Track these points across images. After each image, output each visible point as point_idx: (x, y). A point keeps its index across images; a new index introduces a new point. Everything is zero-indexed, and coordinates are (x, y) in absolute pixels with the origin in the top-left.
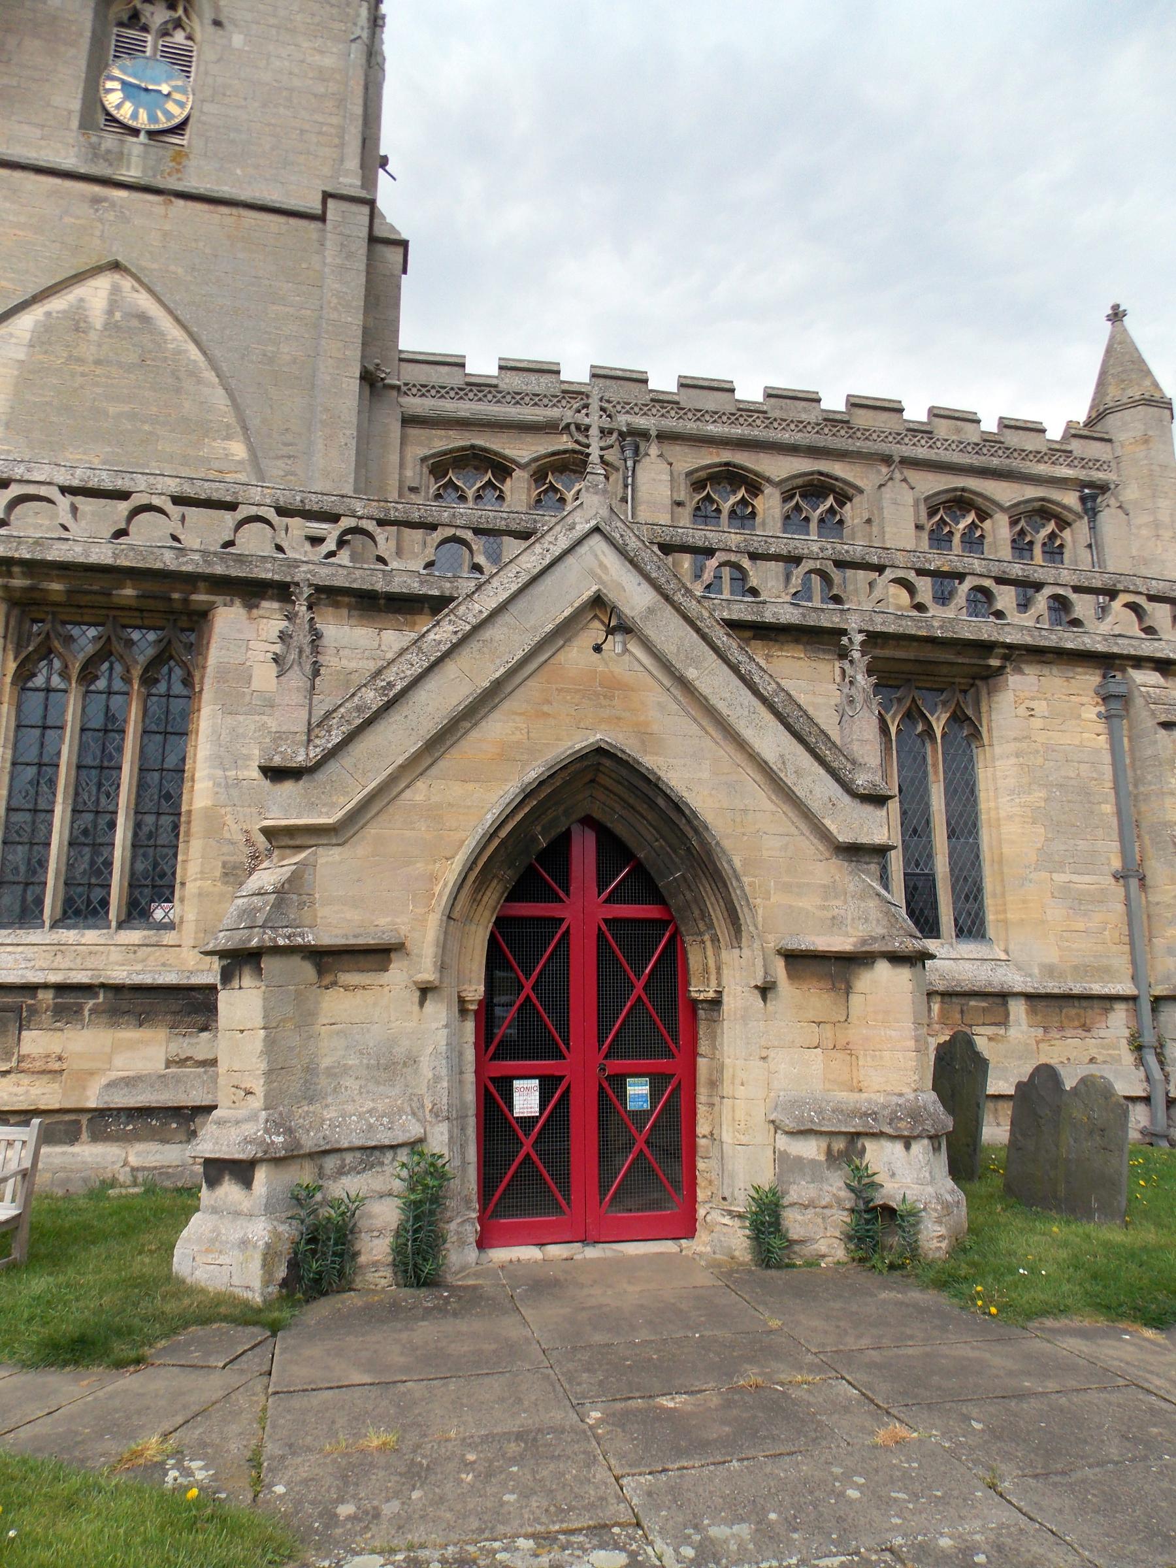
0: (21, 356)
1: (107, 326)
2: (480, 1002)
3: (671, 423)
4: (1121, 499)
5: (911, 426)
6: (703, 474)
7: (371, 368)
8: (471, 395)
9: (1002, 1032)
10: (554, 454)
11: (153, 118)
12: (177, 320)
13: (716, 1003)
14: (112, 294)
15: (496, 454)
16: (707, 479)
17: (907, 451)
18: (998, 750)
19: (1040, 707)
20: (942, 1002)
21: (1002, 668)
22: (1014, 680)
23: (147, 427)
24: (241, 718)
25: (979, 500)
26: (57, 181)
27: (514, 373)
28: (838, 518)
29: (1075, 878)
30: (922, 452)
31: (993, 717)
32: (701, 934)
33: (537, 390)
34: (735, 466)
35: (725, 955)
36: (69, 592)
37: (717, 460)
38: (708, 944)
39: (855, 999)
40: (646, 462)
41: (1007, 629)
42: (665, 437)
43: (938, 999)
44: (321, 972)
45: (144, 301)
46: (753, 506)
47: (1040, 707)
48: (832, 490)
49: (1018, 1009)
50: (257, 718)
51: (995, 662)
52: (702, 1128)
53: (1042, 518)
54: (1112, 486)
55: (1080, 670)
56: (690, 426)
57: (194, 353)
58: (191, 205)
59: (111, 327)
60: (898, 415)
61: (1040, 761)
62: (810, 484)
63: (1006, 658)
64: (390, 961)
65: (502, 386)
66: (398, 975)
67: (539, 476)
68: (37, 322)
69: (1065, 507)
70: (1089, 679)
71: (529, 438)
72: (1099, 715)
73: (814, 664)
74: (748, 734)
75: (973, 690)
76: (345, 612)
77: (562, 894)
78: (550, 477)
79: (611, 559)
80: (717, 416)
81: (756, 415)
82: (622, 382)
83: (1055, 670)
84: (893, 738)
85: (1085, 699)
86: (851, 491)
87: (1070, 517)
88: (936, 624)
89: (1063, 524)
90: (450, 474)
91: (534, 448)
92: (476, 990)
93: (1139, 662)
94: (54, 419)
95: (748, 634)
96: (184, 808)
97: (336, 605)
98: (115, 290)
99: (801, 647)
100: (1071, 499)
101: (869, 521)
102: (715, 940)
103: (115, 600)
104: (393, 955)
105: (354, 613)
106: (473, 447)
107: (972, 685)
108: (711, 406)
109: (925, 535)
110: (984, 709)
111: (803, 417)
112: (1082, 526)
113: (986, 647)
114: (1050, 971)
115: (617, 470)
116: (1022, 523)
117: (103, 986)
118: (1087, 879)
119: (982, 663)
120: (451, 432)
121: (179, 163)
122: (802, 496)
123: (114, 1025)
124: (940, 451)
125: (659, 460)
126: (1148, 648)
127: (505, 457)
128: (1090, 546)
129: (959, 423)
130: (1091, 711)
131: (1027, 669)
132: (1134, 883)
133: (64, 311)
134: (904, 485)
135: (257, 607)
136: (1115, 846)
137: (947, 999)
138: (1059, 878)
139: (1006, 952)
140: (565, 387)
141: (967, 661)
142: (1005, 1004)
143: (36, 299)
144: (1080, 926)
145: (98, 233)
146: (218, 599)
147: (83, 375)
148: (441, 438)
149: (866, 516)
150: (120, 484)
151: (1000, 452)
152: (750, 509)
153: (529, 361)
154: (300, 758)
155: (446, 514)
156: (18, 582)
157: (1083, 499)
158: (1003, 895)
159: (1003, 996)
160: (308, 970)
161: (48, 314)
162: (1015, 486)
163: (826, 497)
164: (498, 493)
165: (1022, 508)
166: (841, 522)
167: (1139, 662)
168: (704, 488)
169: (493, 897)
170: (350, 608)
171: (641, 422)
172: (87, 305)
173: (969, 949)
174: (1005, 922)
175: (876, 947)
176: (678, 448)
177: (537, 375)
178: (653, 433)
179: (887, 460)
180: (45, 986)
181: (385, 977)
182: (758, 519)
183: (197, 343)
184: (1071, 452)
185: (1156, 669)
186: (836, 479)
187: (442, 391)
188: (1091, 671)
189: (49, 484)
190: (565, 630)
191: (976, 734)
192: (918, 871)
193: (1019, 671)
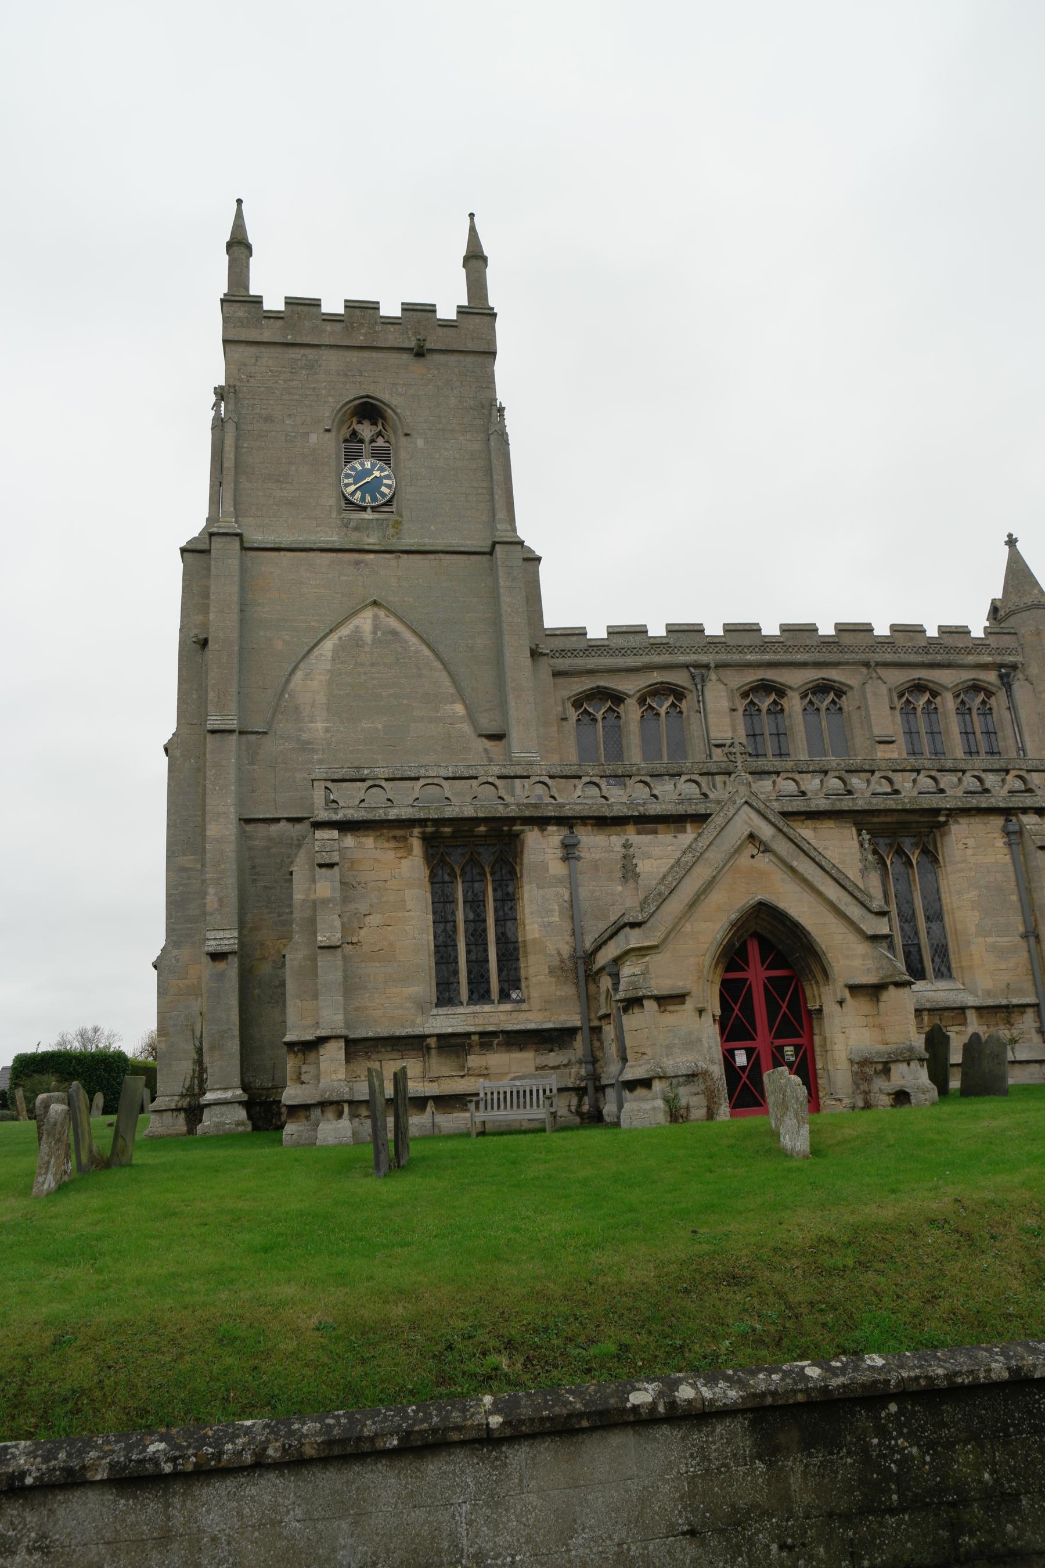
0: (329, 667)
1: (374, 640)
2: (720, 1016)
3: (723, 657)
4: (1027, 673)
5: (880, 640)
6: (747, 688)
7: (534, 647)
8: (593, 653)
9: (964, 1029)
10: (650, 686)
11: (374, 499)
12: (414, 632)
13: (820, 1011)
14: (373, 621)
15: (613, 690)
16: (750, 690)
18: (949, 869)
19: (971, 842)
20: (929, 1015)
21: (946, 823)
23: (405, 702)
24: (546, 890)
25: (931, 685)
26: (334, 555)
27: (618, 635)
28: (838, 706)
29: (999, 939)
30: (889, 657)
31: (945, 850)
32: (810, 981)
33: (634, 645)
34: (767, 680)
35: (822, 989)
36: (453, 832)
37: (755, 678)
38: (814, 985)
39: (882, 1005)
40: (709, 686)
41: (947, 799)
43: (926, 1013)
44: (659, 1006)
45: (393, 623)
46: (782, 705)
47: (971, 842)
48: (832, 688)
49: (971, 1015)
50: (554, 889)
51: (942, 819)
52: (819, 1065)
53: (975, 691)
54: (1020, 666)
55: (991, 818)
56: (736, 657)
57: (427, 652)
58: (411, 556)
59: (376, 641)
61: (973, 874)
62: (818, 686)
63: (947, 816)
64: (685, 1000)
65: (612, 645)
66: (689, 1005)
67: (642, 701)
68: (334, 645)
69: (989, 683)
70: (999, 821)
71: (632, 677)
72: (1005, 843)
73: (841, 831)
74: (822, 888)
75: (932, 834)
76: (589, 828)
77: (765, 966)
78: (648, 700)
79: (754, 815)
81: (777, 645)
82: (688, 633)
83: (977, 819)
84: (889, 867)
85: (996, 835)
86: (845, 689)
87: (994, 689)
88: (907, 801)
89: (989, 694)
90: (585, 705)
91: (636, 683)
92: (718, 1012)
93: (1025, 810)
94: (353, 704)
95: (803, 818)
96: (520, 940)
97: (585, 825)
98: (376, 617)
99: (832, 821)
101: (859, 708)
102: (817, 982)
103: (475, 833)
104: (687, 998)
105: (595, 828)
106: (598, 687)
107: (931, 832)
108: (747, 643)
109: (897, 712)
110: (939, 846)
111: (808, 642)
112: (1002, 694)
113: (937, 811)
114: (988, 993)
115: (691, 691)
116: (962, 696)
117: (502, 1032)
118: (1006, 939)
119: (935, 820)
120: (583, 679)
121: (397, 528)
123: (508, 1051)
124: (902, 655)
125: (718, 683)
126: (1029, 801)
127: (619, 692)
128: (1009, 708)
129: (911, 634)
130: (1000, 842)
132: (1032, 940)
133: (348, 636)
134: (880, 681)
135: (546, 830)
136: (1020, 919)
137: (932, 1013)
138: (990, 940)
139: (963, 984)
140: (652, 641)
141: (926, 820)
142: (964, 1013)
143: (331, 631)
144: (1004, 967)
145: (361, 584)
146: (526, 828)
147: (365, 674)
149: (857, 704)
150: (471, 773)
151: (941, 651)
152: (780, 707)
153: (626, 626)
154: (640, 919)
155: (634, 769)
156: (429, 830)
157: (1001, 677)
158: (959, 952)
159: (962, 1009)
161: (340, 638)
163: (829, 693)
164: (616, 714)
165: (960, 687)
166: (840, 709)
167: (1025, 810)
168: (748, 696)
169: (720, 970)
170: (592, 825)
171: (704, 659)
172: (361, 630)
173: (942, 984)
174: (961, 967)
175: (888, 980)
176: (729, 672)
177: (633, 635)
178: (712, 665)
179: (867, 664)
180: (474, 1033)
181: (684, 1007)
182: (786, 712)
183: (428, 645)
184: (989, 645)
185: (1036, 813)
186: (834, 682)
187: (573, 653)
188: (998, 818)
189: (439, 777)
191: (936, 861)
192: (910, 942)
193: (957, 822)
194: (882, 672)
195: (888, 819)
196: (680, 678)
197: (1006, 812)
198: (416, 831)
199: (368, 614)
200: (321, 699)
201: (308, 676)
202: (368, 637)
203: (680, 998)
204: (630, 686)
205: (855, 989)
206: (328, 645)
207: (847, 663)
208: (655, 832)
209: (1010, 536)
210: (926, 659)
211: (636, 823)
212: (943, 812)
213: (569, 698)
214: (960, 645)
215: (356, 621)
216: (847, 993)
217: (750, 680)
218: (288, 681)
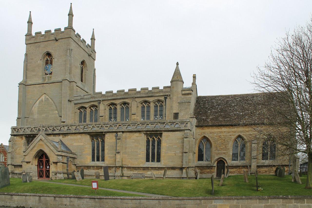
0: (38, 106)
1: (45, 101)
3: (104, 99)
6: (109, 104)
10: (91, 105)
17: (136, 96)
19: (109, 138)
21: (105, 134)
22: (106, 135)
25: (148, 101)
30: (138, 96)
39: (58, 165)
40: (100, 104)
42: (103, 101)
45: (47, 97)
47: (109, 138)
51: (104, 133)
54: (169, 95)
56: (106, 98)
57: (52, 102)
60: (135, 91)
66: (31, 163)
67: (90, 108)
70: (115, 134)
71: (88, 103)
86: (129, 103)
89: (162, 102)
93: (120, 132)
98: (45, 96)
106: (82, 106)
111: (122, 94)
113: (102, 132)
122: (123, 105)
129: (145, 90)
131: (107, 134)
143: (38, 99)
148: (79, 105)
156: (25, 136)
160: (26, 163)
161: (40, 100)
162: (154, 98)
169: (37, 159)
171: (100, 99)
190: (39, 141)
193: (107, 134)
194: (137, 99)
195: (94, 134)
196: (96, 104)
197: (116, 132)
198: (24, 136)
199: (44, 95)
201: (35, 107)
202: (44, 100)
203: (30, 162)
204: (87, 106)
205: (54, 163)
206: (38, 102)
207: (129, 98)
208: (56, 136)
209: (178, 63)
210: (148, 95)
211: (53, 135)
212: (103, 132)
213: (77, 109)
214: (156, 92)
215: (42, 97)
216: (53, 163)
217: (110, 103)
218: (32, 109)
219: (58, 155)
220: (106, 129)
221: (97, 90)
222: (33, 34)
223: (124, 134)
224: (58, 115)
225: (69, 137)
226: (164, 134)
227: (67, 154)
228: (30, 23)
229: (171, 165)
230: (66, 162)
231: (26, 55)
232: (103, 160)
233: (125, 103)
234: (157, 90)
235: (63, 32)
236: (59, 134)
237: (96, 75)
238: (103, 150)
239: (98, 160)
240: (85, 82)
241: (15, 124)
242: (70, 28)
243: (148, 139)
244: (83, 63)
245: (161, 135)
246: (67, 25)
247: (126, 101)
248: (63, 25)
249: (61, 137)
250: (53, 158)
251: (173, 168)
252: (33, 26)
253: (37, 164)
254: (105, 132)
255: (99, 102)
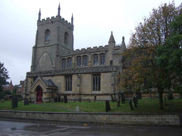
3: (75, 54)
17: (91, 51)
30: (92, 51)
42: (74, 55)
49: (71, 95)
56: (76, 53)
80: (78, 52)
100: (104, 52)
113: (71, 74)
171: (73, 54)
196: (71, 57)
200: (41, 62)
202: (45, 56)
203: (33, 93)
204: (66, 58)
206: (42, 57)
219: (47, 88)
220: (73, 72)
221: (75, 48)
222: (41, 20)
223: (82, 75)
224: (51, 64)
225: (54, 77)
226: (102, 74)
227: (52, 87)
228: (40, 14)
229: (106, 92)
230: (51, 92)
231: (37, 31)
232: (71, 90)
233: (85, 56)
234: (102, 48)
235: (55, 18)
236: (49, 76)
237: (74, 38)
238: (71, 84)
239: (69, 90)
240: (67, 44)
241: (29, 70)
242: (59, 16)
243: (94, 77)
244: (66, 33)
245: (100, 75)
246: (57, 15)
247: (86, 54)
248: (55, 14)
249: (50, 78)
250: (45, 90)
251: (107, 94)
252: (41, 16)
253: (36, 94)
254: (72, 74)
255: (73, 55)
